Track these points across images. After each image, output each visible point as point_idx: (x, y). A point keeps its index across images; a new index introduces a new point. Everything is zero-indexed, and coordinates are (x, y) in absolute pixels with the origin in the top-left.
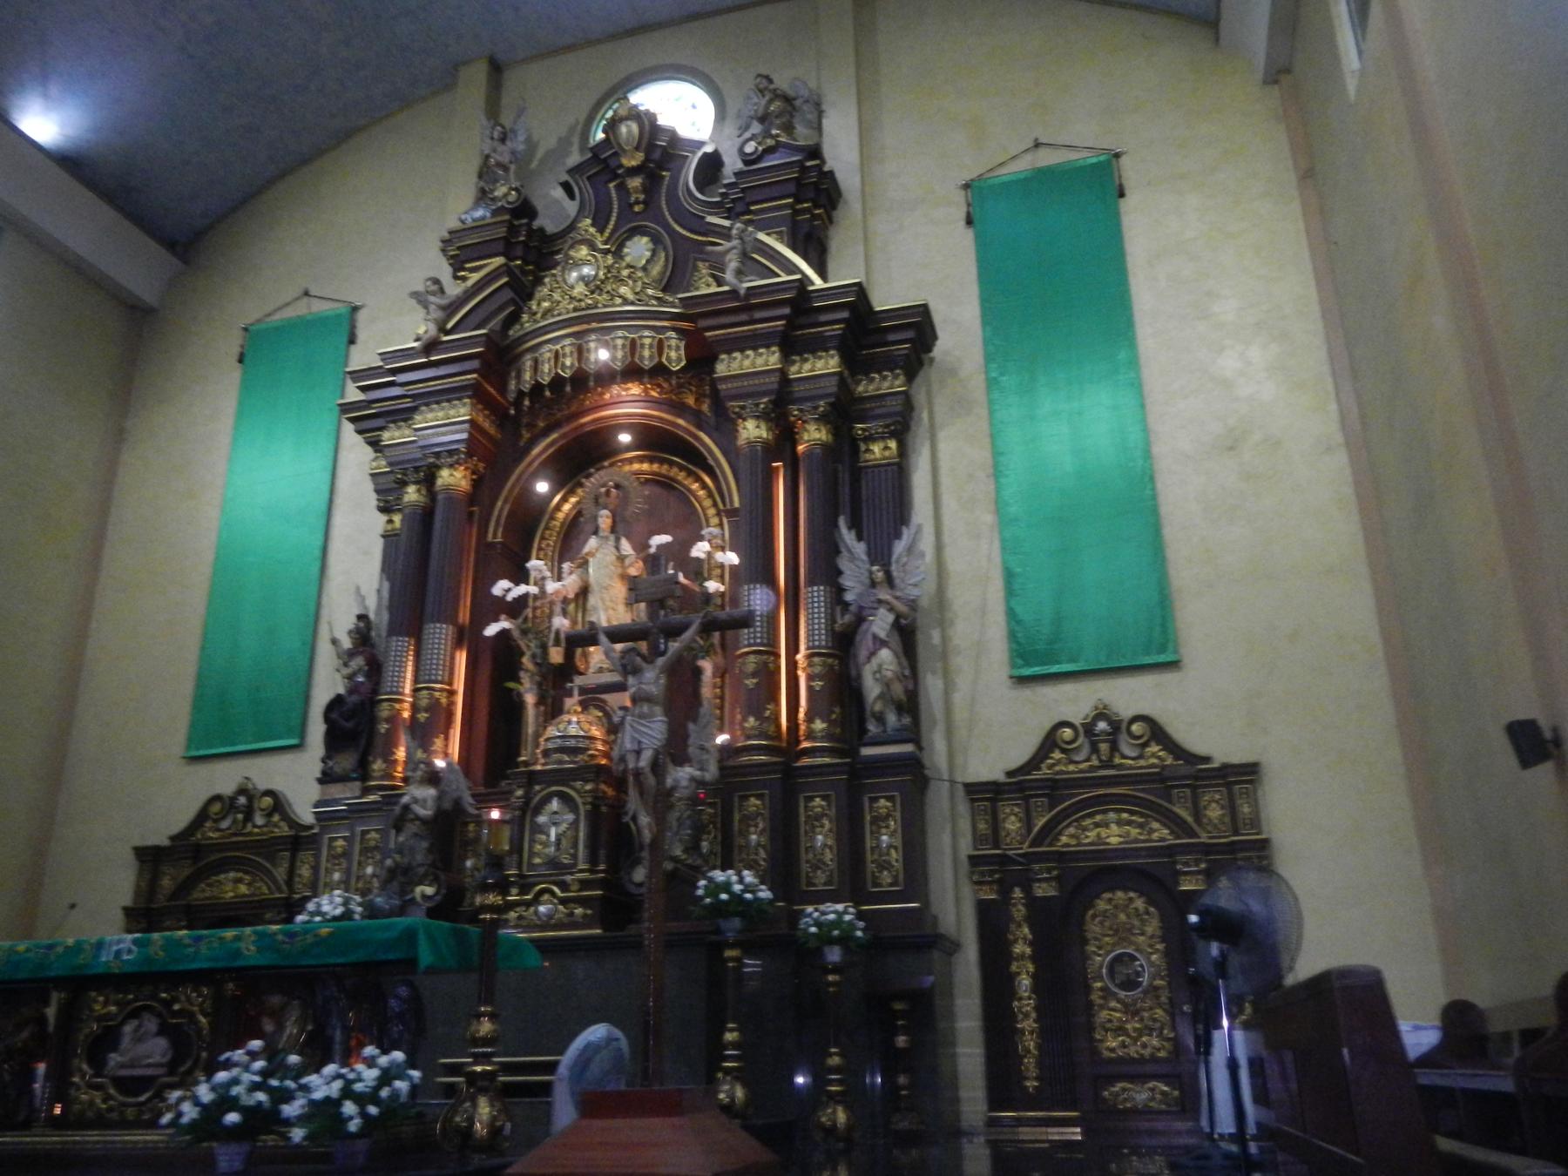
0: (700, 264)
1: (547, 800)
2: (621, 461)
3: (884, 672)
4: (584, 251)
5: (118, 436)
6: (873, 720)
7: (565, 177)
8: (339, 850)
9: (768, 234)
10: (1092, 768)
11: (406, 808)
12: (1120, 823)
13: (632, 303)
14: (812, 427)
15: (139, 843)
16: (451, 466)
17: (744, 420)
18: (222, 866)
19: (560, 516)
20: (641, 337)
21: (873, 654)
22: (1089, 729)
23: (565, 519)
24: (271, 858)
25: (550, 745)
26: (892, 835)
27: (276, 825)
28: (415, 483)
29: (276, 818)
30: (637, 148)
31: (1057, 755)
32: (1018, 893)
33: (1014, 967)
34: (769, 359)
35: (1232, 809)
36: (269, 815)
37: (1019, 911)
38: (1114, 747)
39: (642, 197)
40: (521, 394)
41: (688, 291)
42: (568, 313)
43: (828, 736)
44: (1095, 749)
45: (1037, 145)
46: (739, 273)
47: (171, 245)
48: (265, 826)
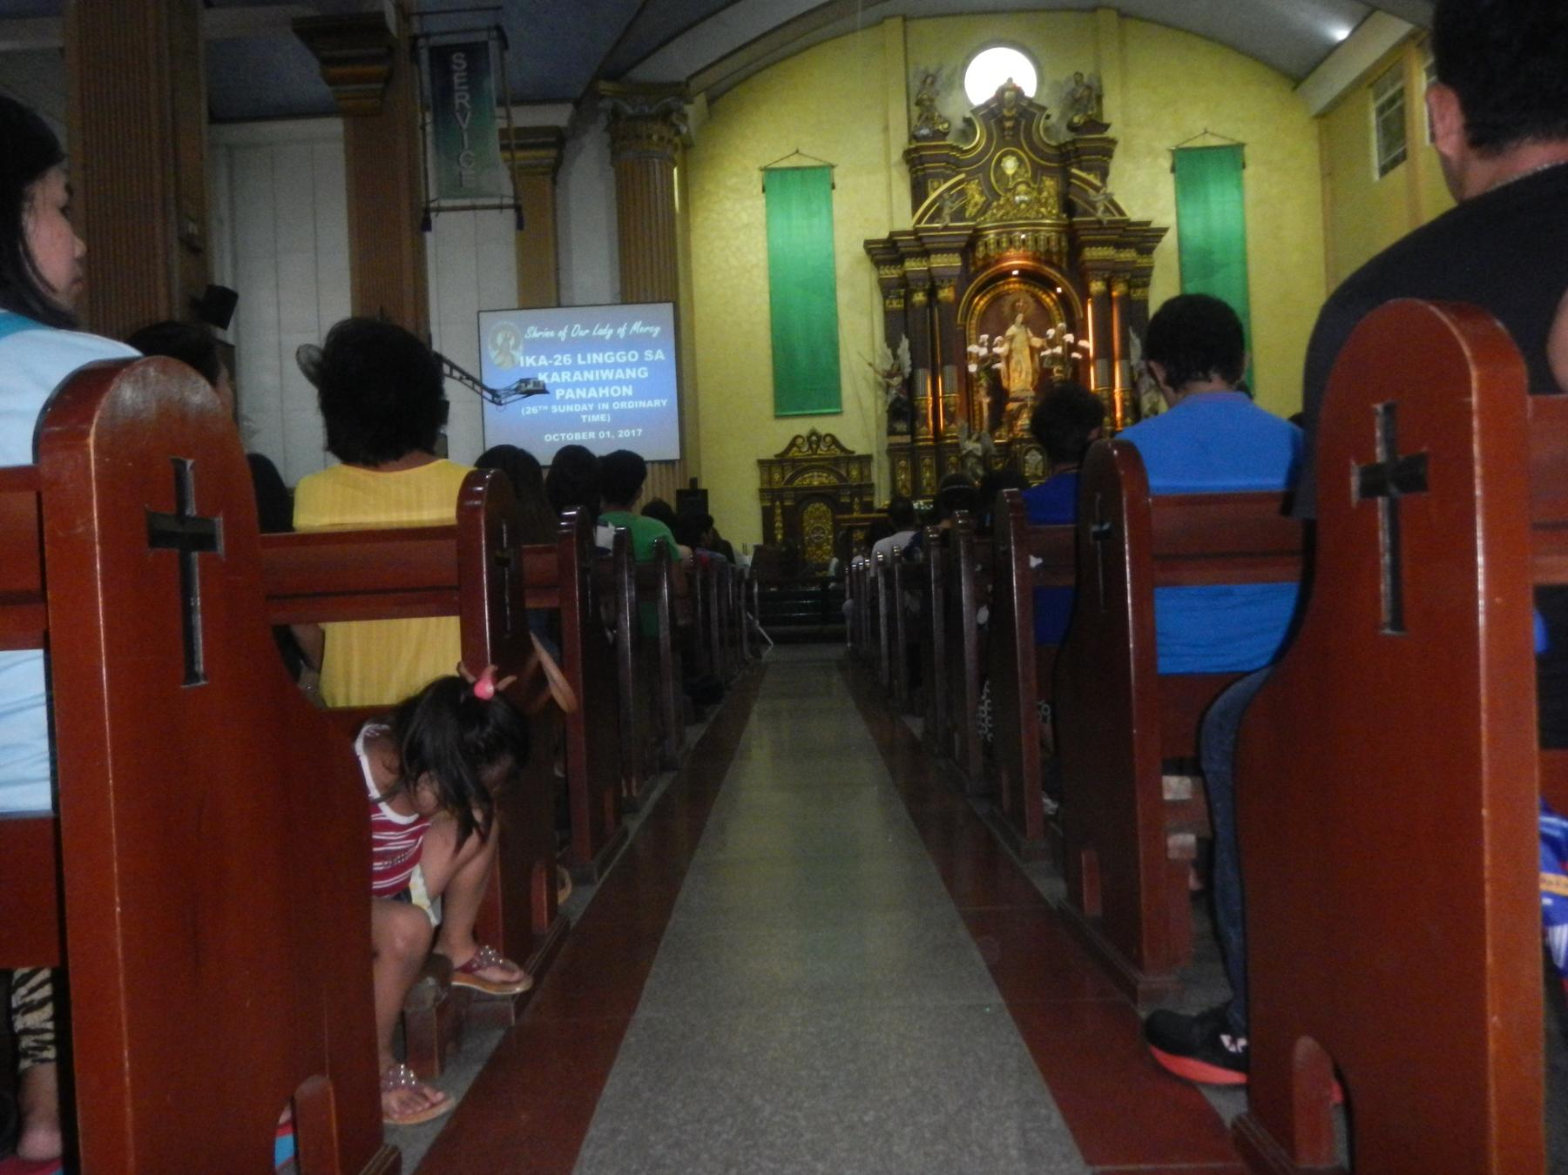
7: (968, 115)
9: (1089, 174)
11: (971, 451)
15: (763, 457)
17: (1097, 281)
18: (806, 470)
19: (978, 308)
23: (981, 309)
27: (833, 449)
28: (924, 290)
29: (833, 447)
40: (987, 256)
45: (1206, 132)
46: (1105, 212)
48: (829, 450)
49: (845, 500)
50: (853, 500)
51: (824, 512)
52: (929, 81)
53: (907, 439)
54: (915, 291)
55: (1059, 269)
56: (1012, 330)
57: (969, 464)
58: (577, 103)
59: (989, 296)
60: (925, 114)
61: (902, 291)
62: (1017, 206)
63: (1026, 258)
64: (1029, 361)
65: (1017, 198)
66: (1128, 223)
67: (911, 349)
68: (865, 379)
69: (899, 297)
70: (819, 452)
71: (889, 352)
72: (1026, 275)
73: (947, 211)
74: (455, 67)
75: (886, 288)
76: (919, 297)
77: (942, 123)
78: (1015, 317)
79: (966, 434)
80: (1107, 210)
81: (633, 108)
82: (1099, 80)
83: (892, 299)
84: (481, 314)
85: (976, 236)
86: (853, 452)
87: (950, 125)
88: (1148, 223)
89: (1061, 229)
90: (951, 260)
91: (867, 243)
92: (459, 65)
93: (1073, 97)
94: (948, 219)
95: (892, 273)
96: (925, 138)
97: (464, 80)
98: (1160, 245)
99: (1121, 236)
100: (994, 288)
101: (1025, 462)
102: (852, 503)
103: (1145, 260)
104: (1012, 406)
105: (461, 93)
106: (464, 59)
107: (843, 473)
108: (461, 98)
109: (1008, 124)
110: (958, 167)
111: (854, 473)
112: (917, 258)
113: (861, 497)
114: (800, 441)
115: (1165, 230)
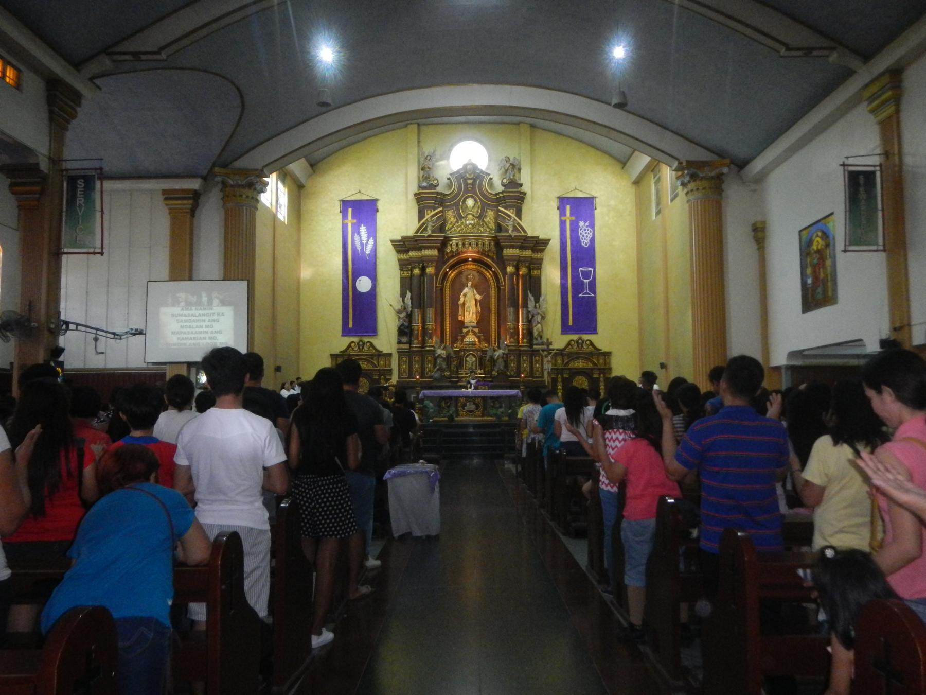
0: (488, 210)
1: (469, 355)
2: (468, 264)
4: (470, 216)
5: (299, 230)
7: (449, 176)
8: (404, 360)
10: (577, 350)
12: (582, 362)
13: (483, 233)
15: (333, 352)
19: (451, 277)
22: (577, 342)
24: (372, 359)
25: (467, 343)
26: (539, 364)
27: (371, 350)
28: (419, 268)
30: (472, 173)
31: (570, 347)
32: (560, 376)
33: (558, 391)
34: (516, 252)
35: (605, 361)
36: (370, 348)
37: (560, 380)
38: (582, 346)
39: (471, 187)
40: (451, 251)
41: (500, 233)
42: (467, 233)
43: (527, 343)
44: (578, 346)
46: (513, 231)
47: (312, 165)
51: (365, 383)
52: (428, 158)
53: (407, 346)
54: (415, 268)
55: (492, 259)
56: (466, 290)
57: (438, 362)
58: (204, 178)
60: (425, 175)
62: (467, 226)
63: (475, 252)
64: (474, 307)
65: (467, 222)
66: (527, 237)
67: (411, 298)
70: (363, 350)
72: (475, 260)
73: (429, 228)
74: (78, 186)
75: (403, 265)
76: (417, 271)
77: (434, 181)
78: (467, 284)
80: (515, 229)
81: (233, 182)
82: (519, 162)
84: (149, 283)
85: (446, 241)
86: (382, 352)
87: (438, 182)
88: (538, 237)
92: (81, 185)
93: (504, 168)
94: (429, 232)
95: (404, 257)
96: (424, 188)
97: (82, 192)
98: (549, 246)
99: (522, 243)
100: (459, 267)
101: (466, 361)
102: (379, 379)
103: (538, 256)
104: (465, 330)
105: (80, 199)
106: (84, 183)
107: (376, 363)
108: (80, 200)
109: (470, 181)
110: (442, 203)
111: (382, 363)
112: (415, 251)
114: (353, 345)
115: (549, 240)
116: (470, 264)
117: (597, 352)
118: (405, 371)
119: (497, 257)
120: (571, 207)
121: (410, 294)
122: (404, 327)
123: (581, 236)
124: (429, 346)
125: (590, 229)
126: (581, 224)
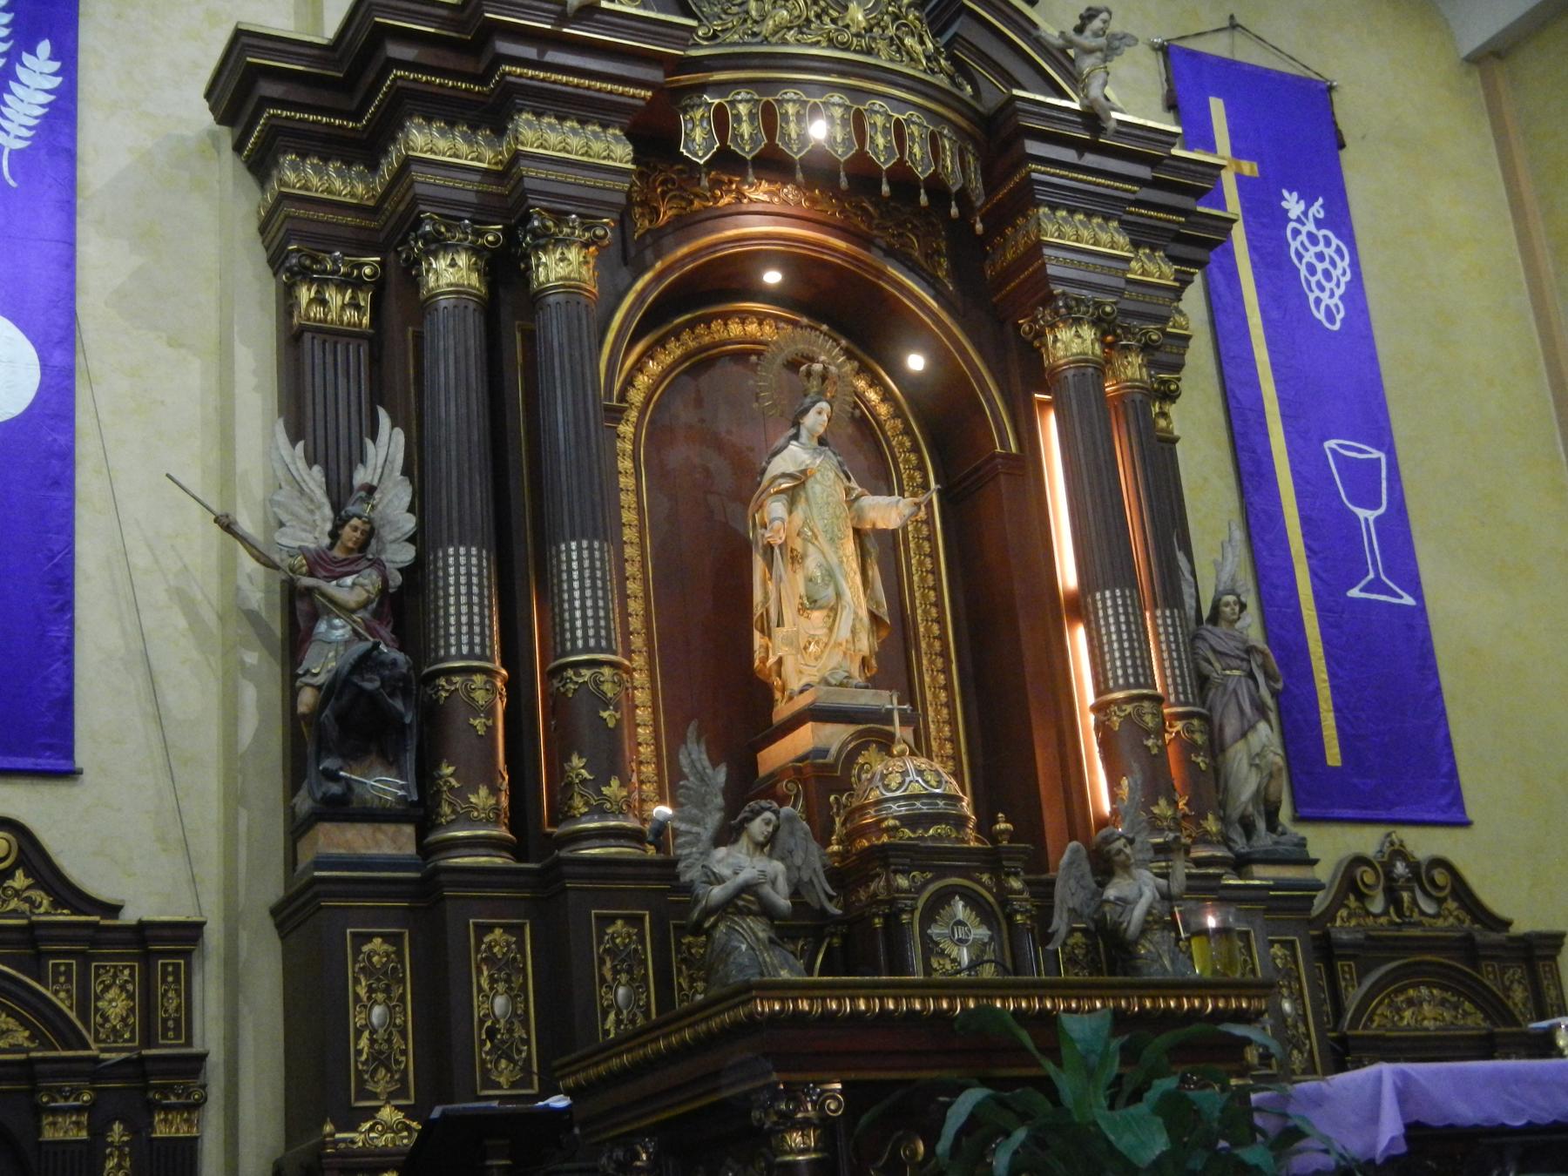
1: (941, 900)
3: (1271, 756)
6: (1239, 829)
14: (1136, 360)
16: (586, 245)
17: (1078, 322)
19: (642, 381)
20: (733, 103)
21: (1252, 727)
27: (17, 893)
28: (475, 250)
34: (1111, 239)
38: (1414, 902)
40: (727, 161)
42: (832, 43)
44: (1393, 898)
45: (1233, 26)
49: (63, 1130)
50: (99, 1131)
53: (396, 842)
56: (793, 457)
59: (675, 350)
61: (369, 265)
67: (406, 471)
68: (182, 598)
69: (351, 282)
71: (314, 479)
79: (714, 819)
83: (326, 281)
86: (114, 910)
89: (963, 123)
90: (597, 146)
91: (242, 40)
100: (691, 325)
107: (62, 1002)
112: (452, 124)
113: (138, 1121)
116: (761, 318)
117: (1494, 937)
118: (380, 1059)
119: (955, 273)
120: (1229, 107)
121: (399, 436)
122: (383, 685)
123: (1303, 272)
124: (604, 835)
125: (1335, 241)
126: (1293, 204)
